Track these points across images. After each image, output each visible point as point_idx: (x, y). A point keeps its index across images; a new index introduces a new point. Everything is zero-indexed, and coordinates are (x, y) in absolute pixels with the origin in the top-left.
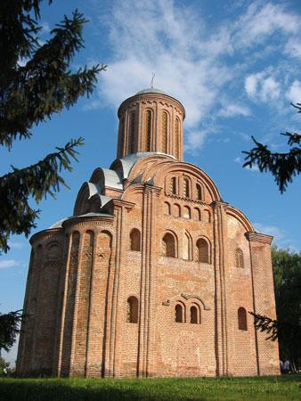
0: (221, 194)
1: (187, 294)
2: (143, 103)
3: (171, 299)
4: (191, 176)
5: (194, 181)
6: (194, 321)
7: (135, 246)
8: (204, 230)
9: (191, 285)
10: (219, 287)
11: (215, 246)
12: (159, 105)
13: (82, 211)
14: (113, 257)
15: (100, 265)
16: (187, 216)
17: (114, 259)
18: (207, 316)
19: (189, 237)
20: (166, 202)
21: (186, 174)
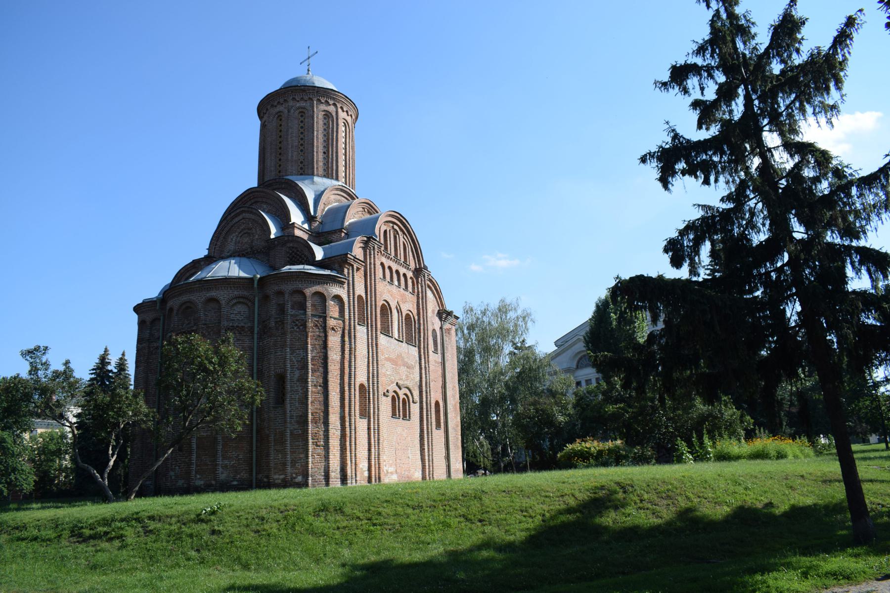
0: (427, 261)
1: (401, 383)
2: (319, 100)
3: (389, 388)
4: (400, 233)
5: (401, 239)
6: (405, 416)
7: (362, 321)
8: (409, 306)
9: (403, 370)
10: (424, 376)
11: (419, 323)
12: (340, 110)
13: (231, 246)
14: (346, 332)
15: (334, 340)
16: (396, 283)
17: (347, 336)
18: (415, 409)
19: (399, 311)
20: (382, 264)
21: (395, 227)
